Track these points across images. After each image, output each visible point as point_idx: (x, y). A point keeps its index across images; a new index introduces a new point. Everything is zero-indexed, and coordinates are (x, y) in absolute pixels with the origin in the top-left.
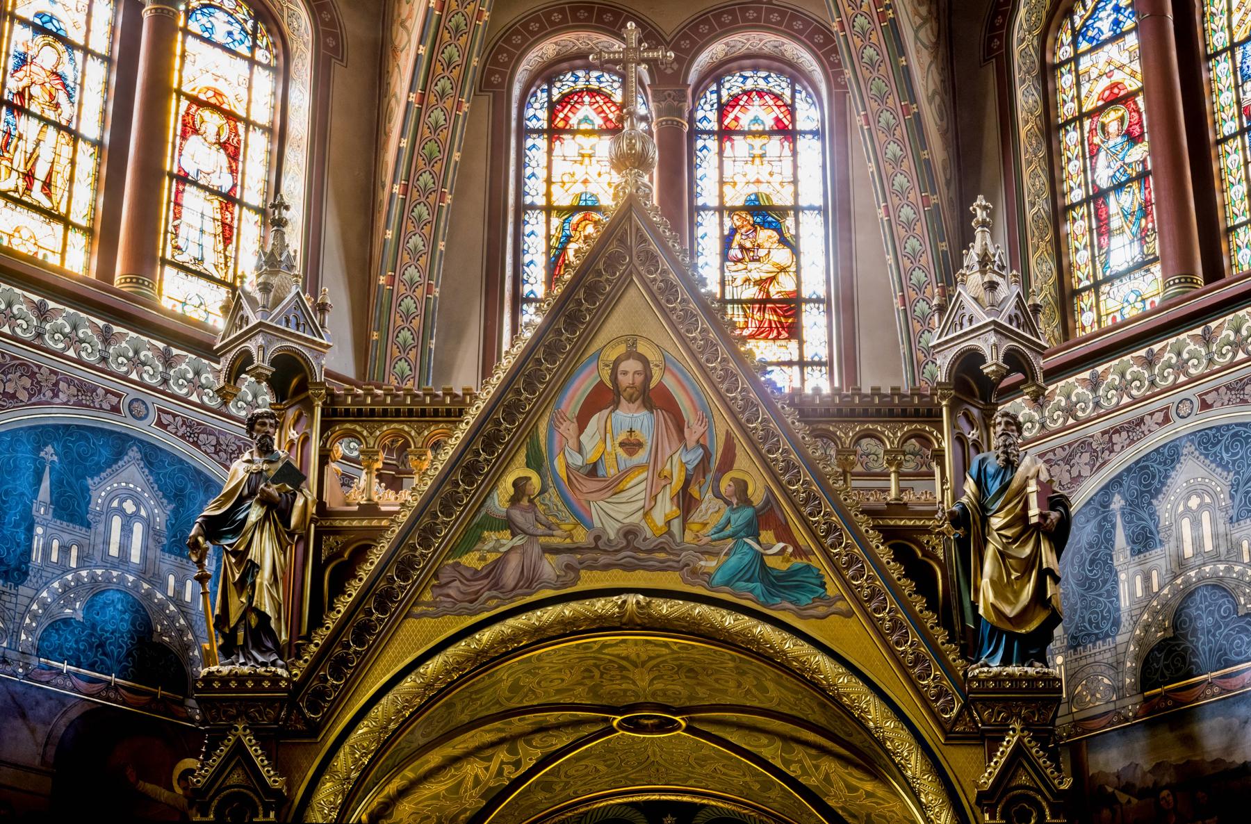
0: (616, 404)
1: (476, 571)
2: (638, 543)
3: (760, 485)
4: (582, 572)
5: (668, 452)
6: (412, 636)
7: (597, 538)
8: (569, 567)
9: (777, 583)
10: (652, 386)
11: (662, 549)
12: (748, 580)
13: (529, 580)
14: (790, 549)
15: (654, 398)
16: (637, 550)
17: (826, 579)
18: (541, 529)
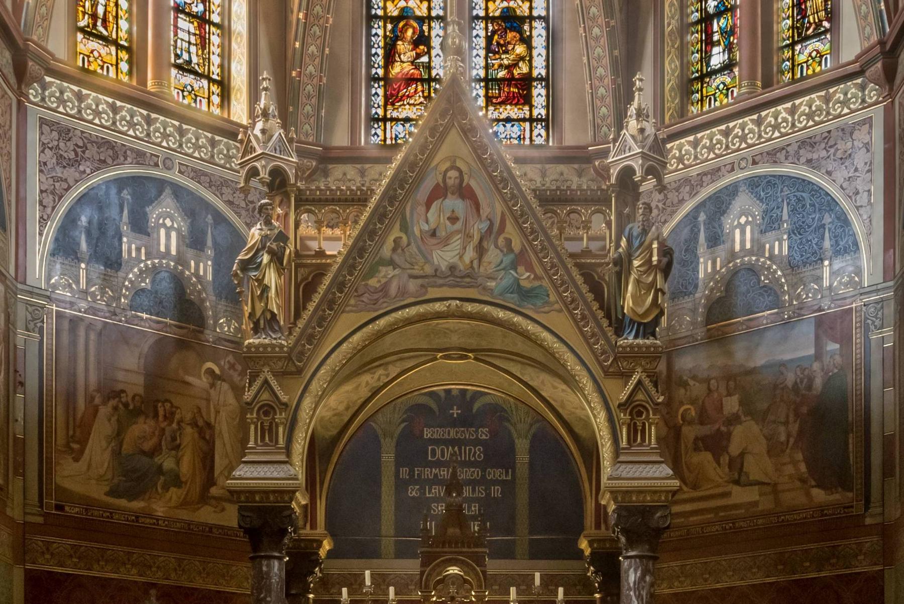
0: (445, 197)
1: (376, 288)
2: (457, 273)
3: (518, 241)
4: (429, 289)
5: (472, 223)
7: (436, 270)
8: (422, 286)
10: (464, 184)
11: (469, 276)
12: (511, 293)
13: (402, 292)
14: (532, 276)
15: (465, 193)
16: (457, 277)
17: (550, 292)
18: (408, 266)
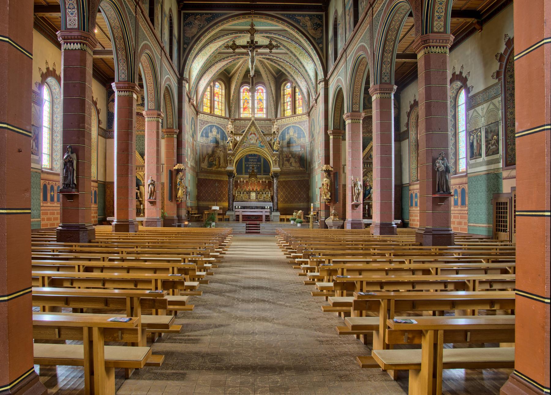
6: (240, 149)
9: (262, 146)
15: (254, 134)
